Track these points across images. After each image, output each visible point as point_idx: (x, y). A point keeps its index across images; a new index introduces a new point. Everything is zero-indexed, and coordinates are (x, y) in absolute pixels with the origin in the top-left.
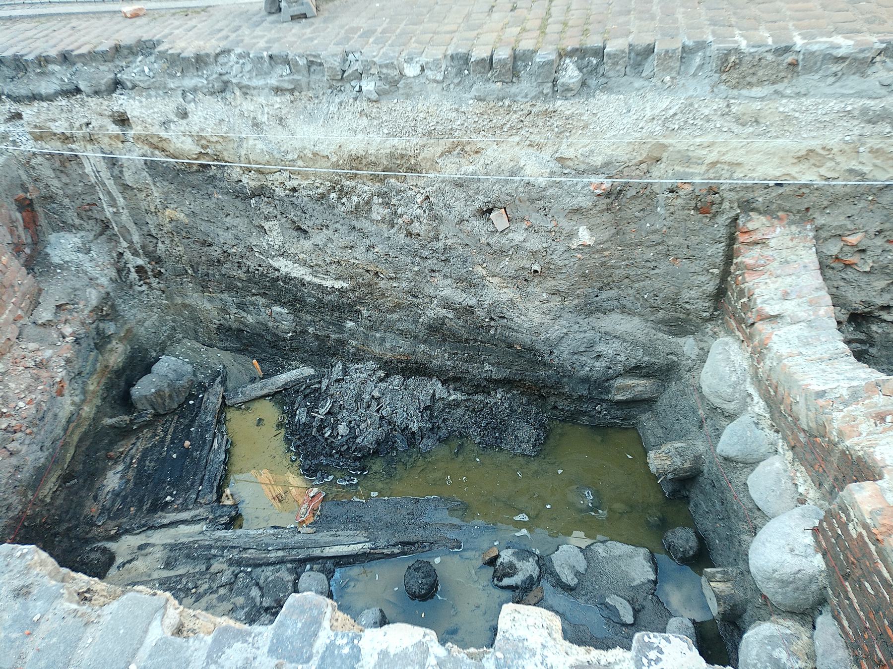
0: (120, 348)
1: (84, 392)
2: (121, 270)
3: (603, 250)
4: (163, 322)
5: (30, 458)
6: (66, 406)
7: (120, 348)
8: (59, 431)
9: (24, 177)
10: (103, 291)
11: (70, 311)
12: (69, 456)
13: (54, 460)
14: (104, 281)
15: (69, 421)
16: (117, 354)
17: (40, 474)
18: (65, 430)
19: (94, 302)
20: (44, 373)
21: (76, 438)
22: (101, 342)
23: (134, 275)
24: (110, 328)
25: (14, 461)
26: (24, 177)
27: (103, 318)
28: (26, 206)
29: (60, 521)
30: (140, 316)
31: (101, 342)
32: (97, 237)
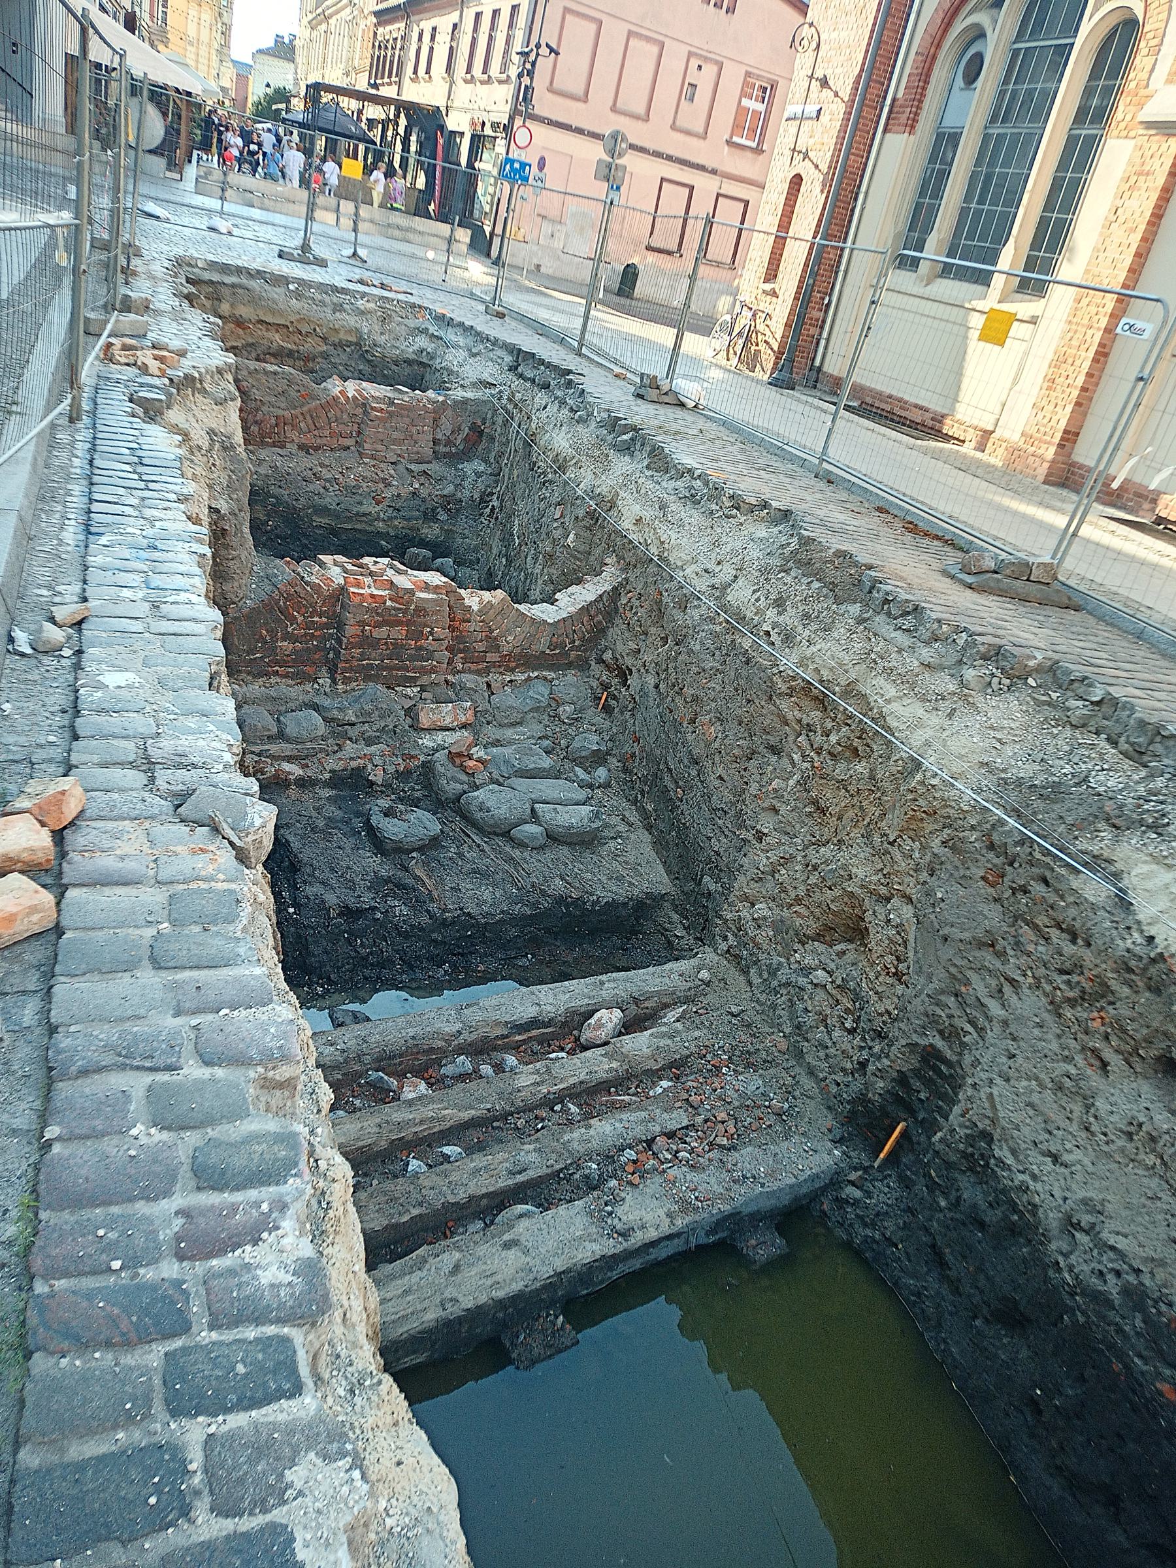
0: (437, 531)
1: (390, 519)
2: (484, 498)
3: (575, 558)
4: (476, 550)
5: (329, 500)
6: (373, 509)
7: (437, 531)
8: (355, 510)
9: (489, 416)
10: (459, 495)
11: (431, 484)
12: (345, 526)
13: (336, 515)
14: (466, 493)
15: (364, 515)
16: (431, 532)
17: (324, 511)
18: (357, 514)
19: (445, 492)
20: (381, 485)
21: (359, 526)
22: (429, 516)
23: (488, 510)
24: (443, 516)
25: (322, 490)
26: (489, 416)
27: (445, 508)
28: (477, 433)
29: (307, 537)
30: (466, 532)
31: (429, 516)
32: (491, 475)
